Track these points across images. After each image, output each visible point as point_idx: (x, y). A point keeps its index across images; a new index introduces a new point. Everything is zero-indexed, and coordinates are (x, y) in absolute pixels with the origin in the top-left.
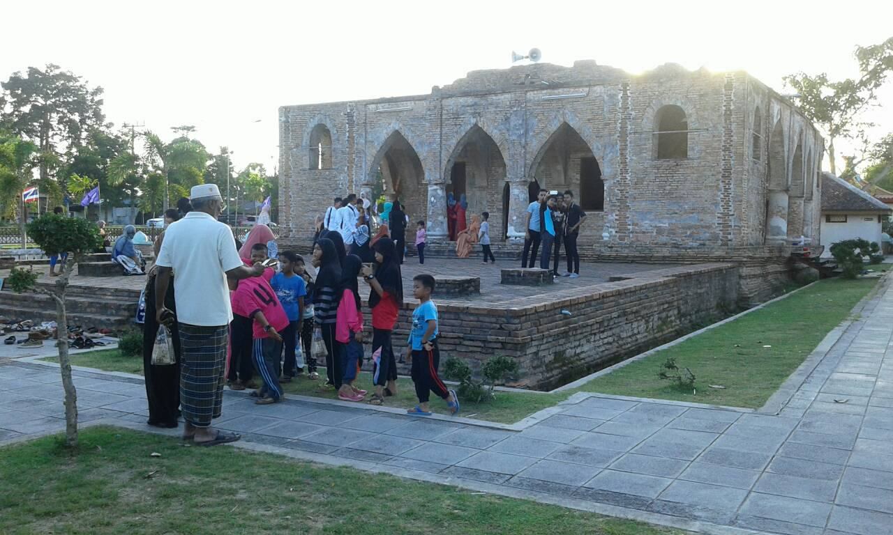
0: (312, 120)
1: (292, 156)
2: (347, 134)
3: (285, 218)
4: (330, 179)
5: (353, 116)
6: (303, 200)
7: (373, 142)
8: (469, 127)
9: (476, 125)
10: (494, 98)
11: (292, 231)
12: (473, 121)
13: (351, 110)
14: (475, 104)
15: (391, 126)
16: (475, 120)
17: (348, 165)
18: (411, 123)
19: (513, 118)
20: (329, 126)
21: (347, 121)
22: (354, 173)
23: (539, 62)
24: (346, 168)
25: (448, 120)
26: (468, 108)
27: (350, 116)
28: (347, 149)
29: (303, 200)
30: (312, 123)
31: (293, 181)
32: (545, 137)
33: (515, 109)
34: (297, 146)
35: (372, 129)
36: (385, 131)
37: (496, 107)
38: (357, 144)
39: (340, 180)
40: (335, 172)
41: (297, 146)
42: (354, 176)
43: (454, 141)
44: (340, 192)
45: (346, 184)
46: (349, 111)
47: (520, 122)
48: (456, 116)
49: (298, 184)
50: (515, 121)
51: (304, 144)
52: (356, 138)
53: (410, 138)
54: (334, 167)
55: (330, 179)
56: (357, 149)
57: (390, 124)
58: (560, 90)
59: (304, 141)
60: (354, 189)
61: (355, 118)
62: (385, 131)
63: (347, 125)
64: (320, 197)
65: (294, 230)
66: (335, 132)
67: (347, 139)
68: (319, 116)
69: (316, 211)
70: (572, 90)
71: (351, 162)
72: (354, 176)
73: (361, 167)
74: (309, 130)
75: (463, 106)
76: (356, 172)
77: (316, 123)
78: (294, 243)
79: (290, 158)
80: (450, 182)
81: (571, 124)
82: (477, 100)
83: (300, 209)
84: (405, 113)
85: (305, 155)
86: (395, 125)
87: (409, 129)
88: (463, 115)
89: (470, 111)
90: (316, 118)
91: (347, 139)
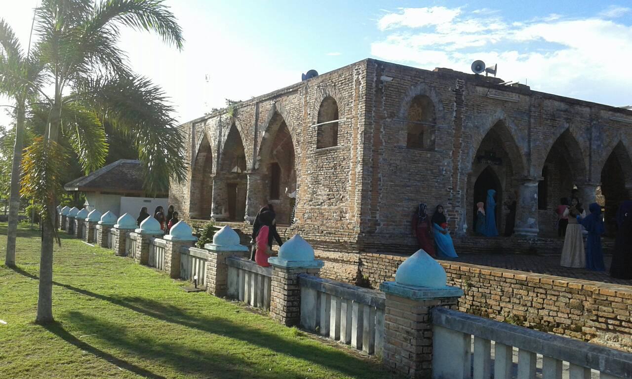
0: (412, 87)
1: (384, 128)
2: (454, 114)
3: (370, 207)
4: (432, 164)
5: (462, 95)
6: (397, 186)
7: (478, 128)
8: (563, 130)
9: (568, 129)
10: (580, 109)
11: (379, 225)
12: (567, 125)
13: (461, 87)
14: (565, 111)
15: (496, 114)
16: (568, 124)
17: (454, 149)
18: (515, 116)
19: (593, 130)
20: (434, 99)
21: (455, 99)
22: (459, 158)
23: (497, 77)
24: (451, 153)
25: (547, 120)
26: (562, 113)
27: (458, 93)
28: (454, 131)
29: (397, 186)
30: (413, 92)
31: (384, 159)
32: (610, 150)
33: (595, 122)
34: (392, 115)
35: (478, 113)
36: (490, 119)
37: (581, 117)
38: (465, 127)
39: (444, 165)
40: (438, 156)
41: (392, 115)
42: (459, 163)
43: (551, 141)
44: (443, 179)
45: (450, 171)
46: (458, 88)
47: (598, 134)
48: (553, 118)
49: (390, 165)
50: (595, 133)
51: (401, 115)
52: (463, 120)
53: (513, 130)
54: (436, 149)
55: (432, 164)
56: (464, 133)
57: (495, 112)
58: (619, 114)
59: (402, 111)
60: (458, 177)
61: (463, 97)
62: (490, 119)
63: (455, 104)
64: (419, 184)
65: (382, 224)
66: (441, 109)
67: (453, 119)
68: (422, 84)
69: (413, 200)
70: (625, 116)
71: (457, 146)
72: (459, 163)
73: (468, 153)
74: (408, 99)
75: (557, 110)
76: (462, 159)
77: (419, 93)
78: (390, 241)
79: (382, 130)
80: (542, 179)
81: (624, 142)
82: (567, 107)
83: (393, 196)
84: (510, 104)
85: (402, 129)
86: (500, 114)
87: (513, 121)
88: (558, 117)
89: (564, 116)
90: (419, 88)
91: (453, 119)
